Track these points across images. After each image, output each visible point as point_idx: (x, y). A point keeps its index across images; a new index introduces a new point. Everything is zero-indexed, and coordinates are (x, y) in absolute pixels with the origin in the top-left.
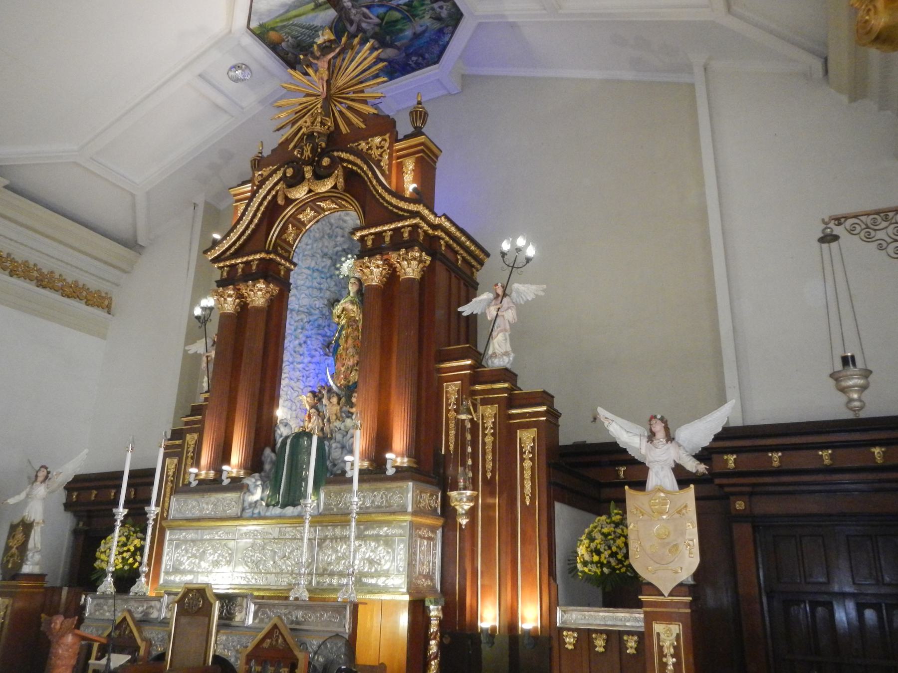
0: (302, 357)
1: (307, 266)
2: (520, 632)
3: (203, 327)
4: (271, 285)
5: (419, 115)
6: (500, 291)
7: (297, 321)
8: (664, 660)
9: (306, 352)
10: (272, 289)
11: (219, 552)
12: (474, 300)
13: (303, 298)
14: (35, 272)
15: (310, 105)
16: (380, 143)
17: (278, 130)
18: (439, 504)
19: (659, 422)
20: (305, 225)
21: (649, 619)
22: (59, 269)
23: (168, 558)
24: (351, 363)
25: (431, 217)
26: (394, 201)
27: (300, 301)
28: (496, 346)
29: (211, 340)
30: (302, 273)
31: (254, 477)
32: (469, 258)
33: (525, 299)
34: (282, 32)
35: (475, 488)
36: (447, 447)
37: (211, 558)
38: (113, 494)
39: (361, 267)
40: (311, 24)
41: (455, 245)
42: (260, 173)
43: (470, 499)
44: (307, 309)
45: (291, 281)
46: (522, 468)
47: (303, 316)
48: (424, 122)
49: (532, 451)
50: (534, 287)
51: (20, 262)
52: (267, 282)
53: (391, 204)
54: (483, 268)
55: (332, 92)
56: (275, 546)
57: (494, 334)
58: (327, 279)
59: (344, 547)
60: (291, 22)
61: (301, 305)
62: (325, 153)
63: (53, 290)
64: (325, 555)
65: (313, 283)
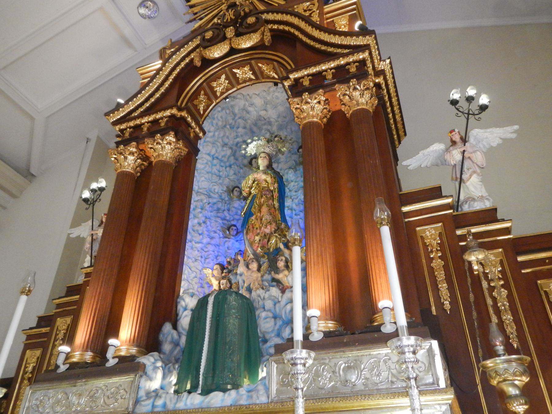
0: (201, 236)
1: (208, 152)
4: (181, 142)
6: (457, 138)
7: (197, 201)
9: (205, 232)
13: (203, 181)
16: (308, 7)
20: (216, 98)
24: (268, 231)
27: (200, 183)
28: (472, 188)
29: (97, 221)
30: (202, 158)
31: (152, 356)
33: (487, 146)
36: (440, 305)
44: (206, 191)
47: (203, 197)
57: (464, 177)
58: (226, 168)
61: (200, 187)
65: (212, 169)
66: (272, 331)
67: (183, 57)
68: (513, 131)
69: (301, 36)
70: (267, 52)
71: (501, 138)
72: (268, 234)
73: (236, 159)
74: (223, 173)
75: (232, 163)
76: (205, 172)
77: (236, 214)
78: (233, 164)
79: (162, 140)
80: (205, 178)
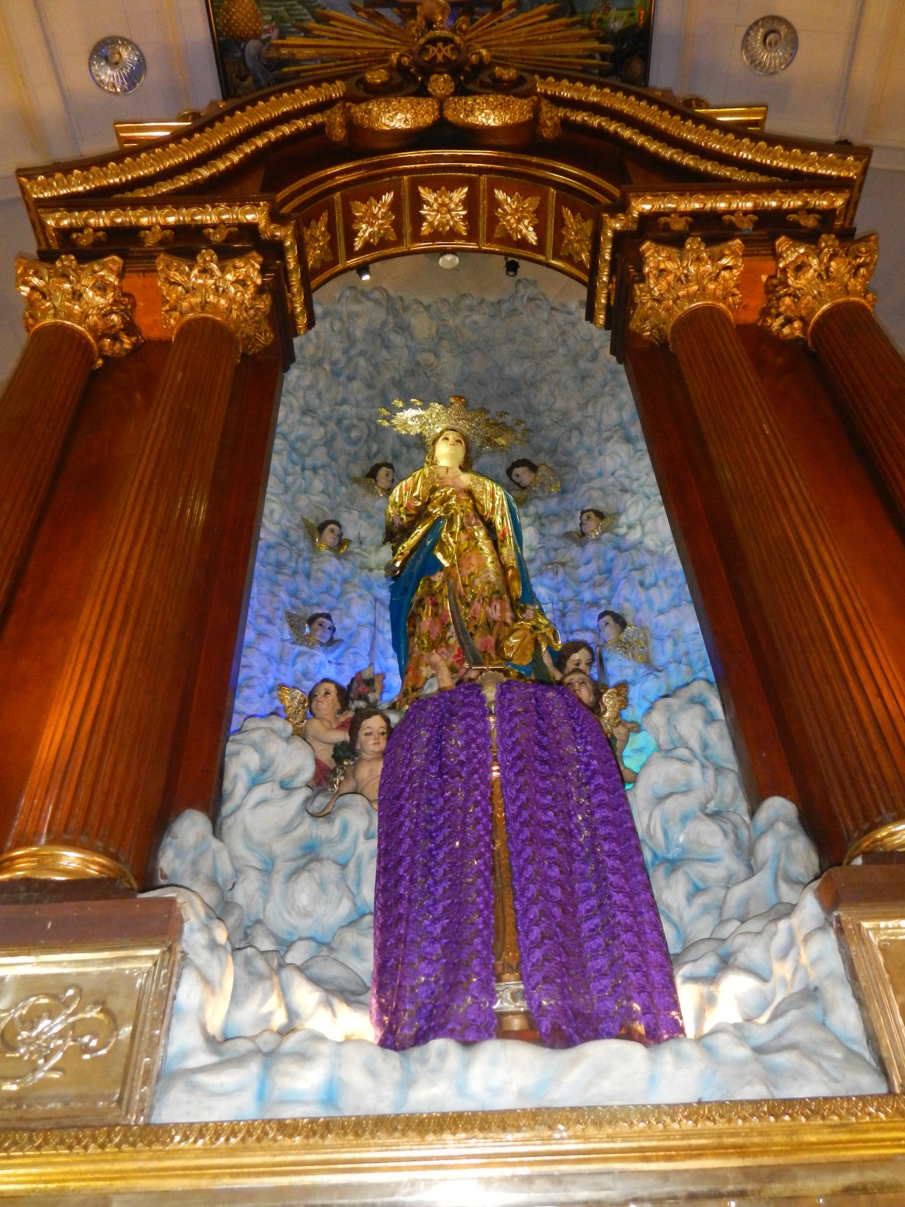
34: (265, 9)
67: (284, 113)
69: (640, 140)
70: (535, 160)
72: (495, 622)
73: (333, 458)
75: (318, 463)
77: (328, 590)
78: (323, 467)
79: (223, 270)
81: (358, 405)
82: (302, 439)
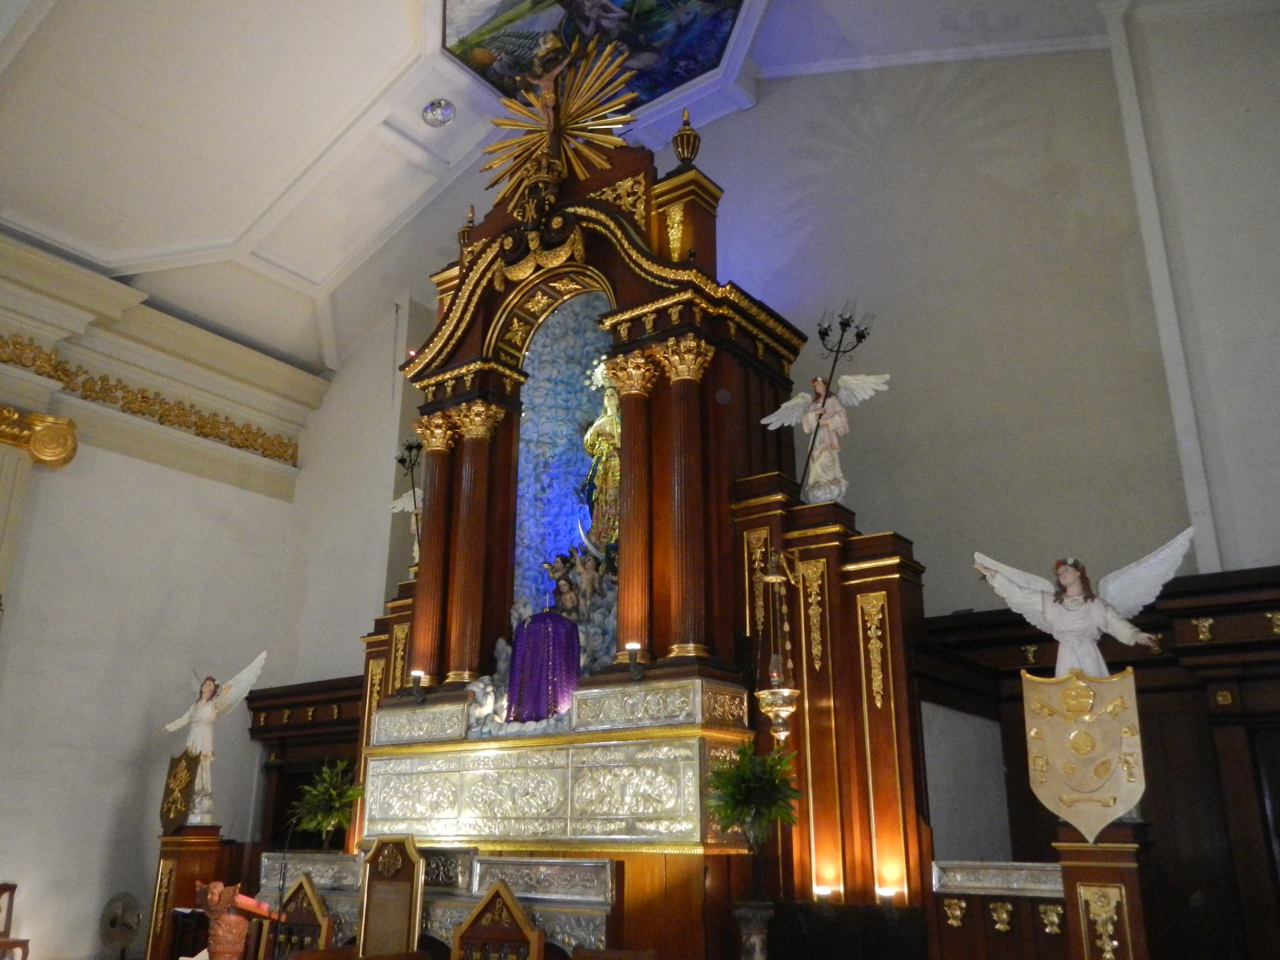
1: (547, 377)
2: (878, 902)
3: (410, 475)
4: (493, 407)
5: (689, 141)
6: (821, 389)
8: (1099, 943)
10: (495, 413)
11: (439, 789)
12: (784, 405)
13: (543, 423)
14: (193, 416)
15: (533, 145)
16: (632, 187)
17: (492, 186)
18: (746, 710)
19: (1071, 569)
20: (537, 318)
21: (1071, 878)
22: (225, 408)
23: (372, 800)
25: (709, 288)
26: (655, 269)
27: (540, 428)
30: (539, 387)
32: (774, 344)
33: (860, 399)
35: (798, 685)
37: (429, 798)
38: (310, 713)
39: (614, 369)
40: (531, 31)
41: (750, 328)
42: (470, 249)
43: (788, 701)
44: (550, 438)
45: (524, 398)
46: (867, 652)
47: (545, 448)
48: (694, 151)
49: (881, 626)
50: (872, 379)
51: (172, 403)
52: (487, 402)
53: (651, 274)
54: (800, 357)
55: (563, 122)
56: (513, 778)
57: (815, 453)
58: (576, 393)
59: (609, 777)
60: (503, 31)
61: (541, 433)
62: (556, 209)
63: (217, 439)
64: (583, 790)
65: (556, 401)
66: (601, 649)
68: (884, 381)
71: (874, 390)
74: (573, 403)
76: (546, 409)
80: (547, 418)
81: (593, 344)
82: (571, 376)
